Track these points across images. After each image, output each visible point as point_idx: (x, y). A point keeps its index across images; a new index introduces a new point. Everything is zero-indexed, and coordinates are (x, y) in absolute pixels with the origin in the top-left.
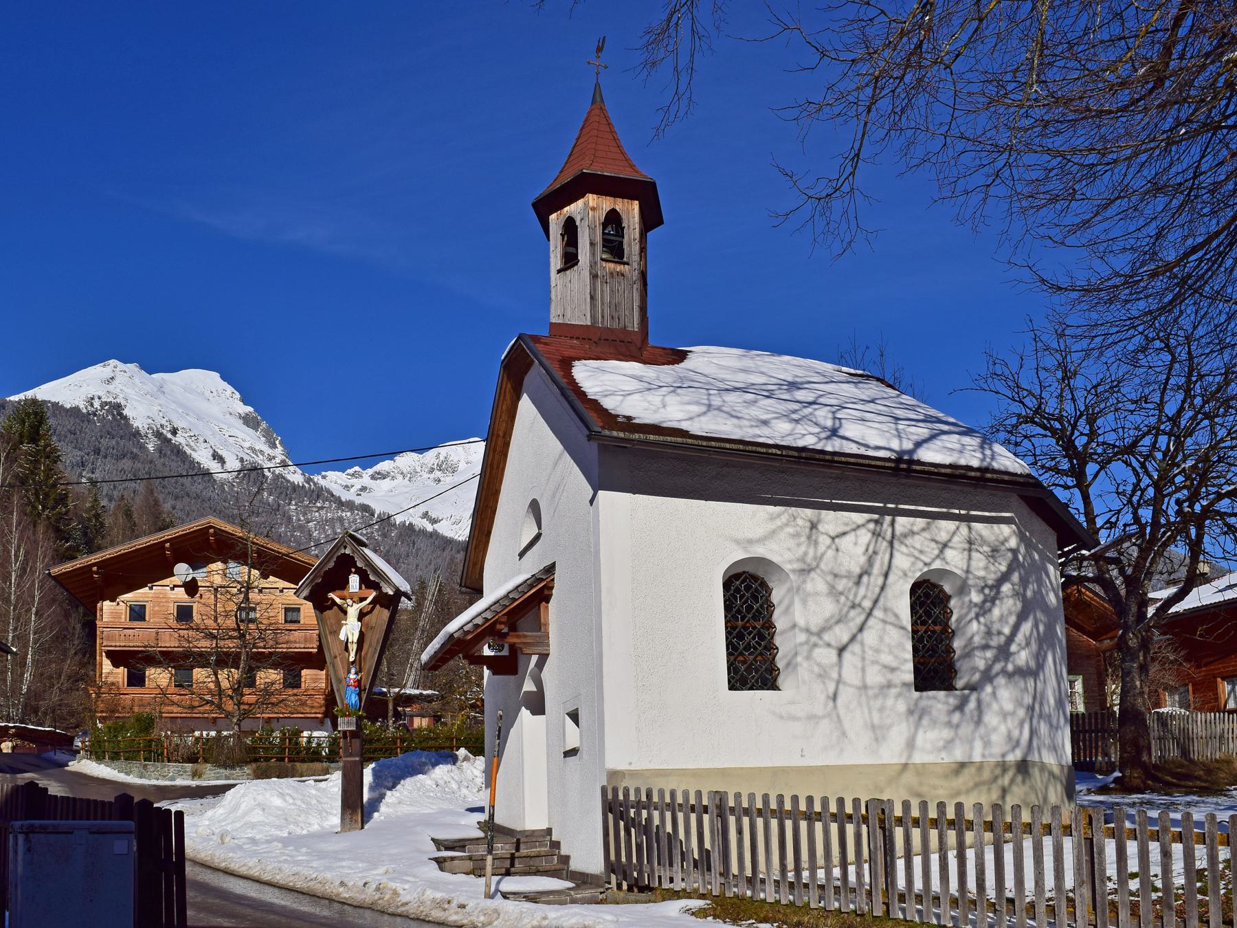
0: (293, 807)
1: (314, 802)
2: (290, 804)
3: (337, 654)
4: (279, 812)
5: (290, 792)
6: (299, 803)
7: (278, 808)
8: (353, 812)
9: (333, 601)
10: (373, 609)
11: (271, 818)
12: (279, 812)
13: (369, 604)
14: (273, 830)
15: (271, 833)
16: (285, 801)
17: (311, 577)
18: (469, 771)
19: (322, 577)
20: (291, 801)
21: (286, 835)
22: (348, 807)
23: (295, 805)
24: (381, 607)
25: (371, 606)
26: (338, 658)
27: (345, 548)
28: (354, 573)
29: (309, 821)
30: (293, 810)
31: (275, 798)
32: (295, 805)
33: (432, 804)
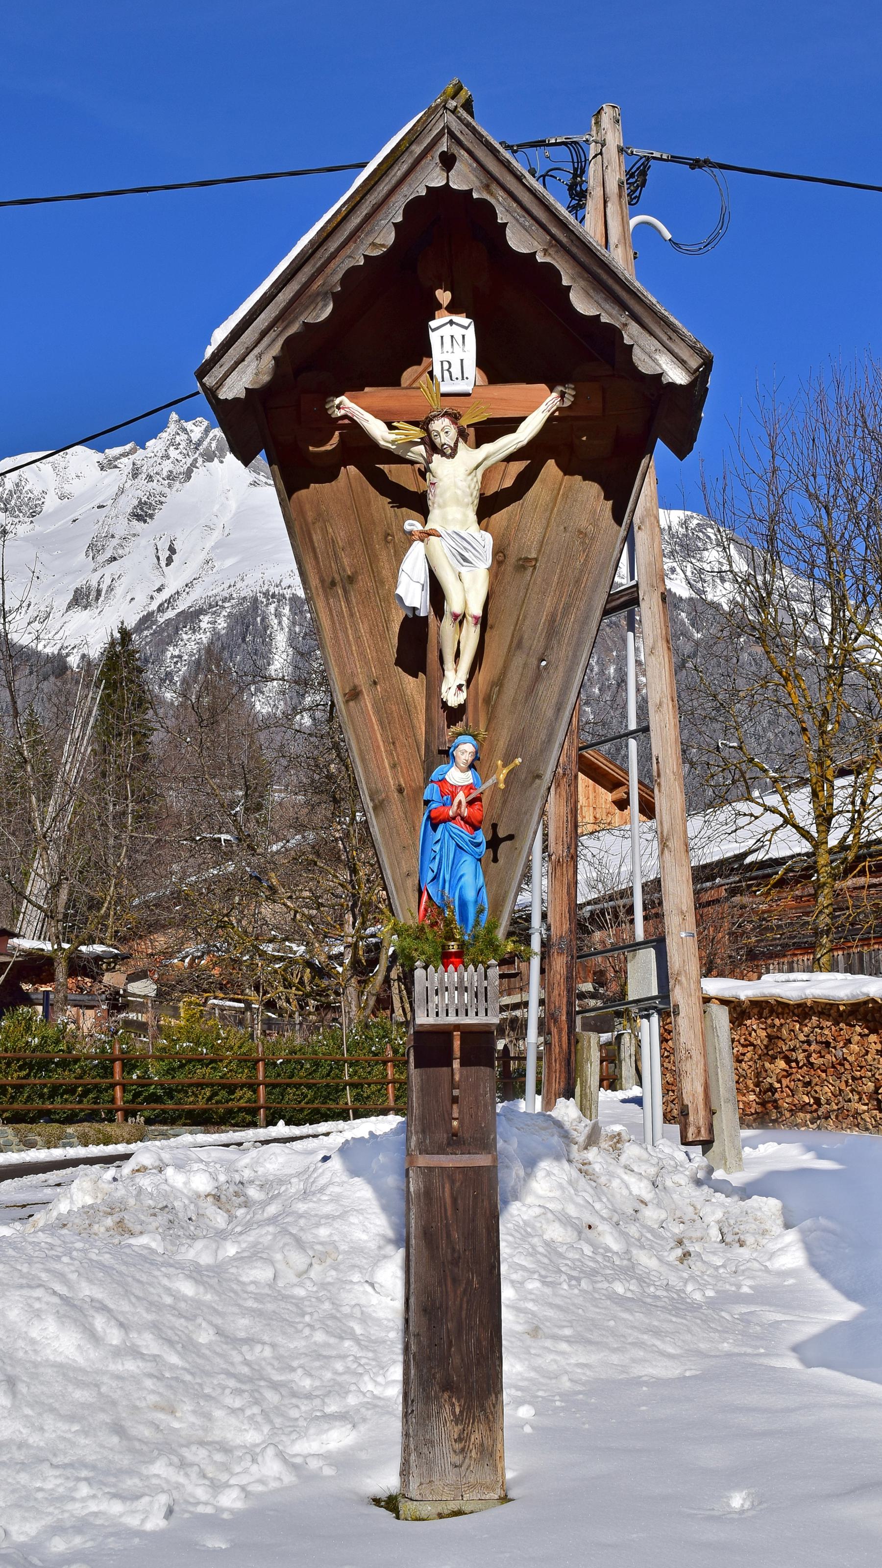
0: (131, 1366)
1: (205, 1336)
2: (117, 1353)
3: (362, 681)
4: (80, 1395)
5: (98, 1293)
6: (149, 1343)
7: (66, 1371)
8: (467, 1409)
9: (354, 428)
10: (525, 481)
11: (54, 1428)
12: (80, 1395)
13: (510, 458)
14: (84, 1490)
15: (76, 1508)
16: (94, 1337)
17: (283, 298)
18: (616, 1183)
19: (336, 297)
20: (114, 1336)
21: (156, 1522)
22: (448, 1386)
23: (135, 1353)
24: (567, 470)
25: (518, 467)
26: (367, 700)
27: (448, 162)
28: (453, 308)
29: (216, 1435)
30: (135, 1379)
31: (51, 1325)
32: (135, 1353)
33: (657, 1333)
